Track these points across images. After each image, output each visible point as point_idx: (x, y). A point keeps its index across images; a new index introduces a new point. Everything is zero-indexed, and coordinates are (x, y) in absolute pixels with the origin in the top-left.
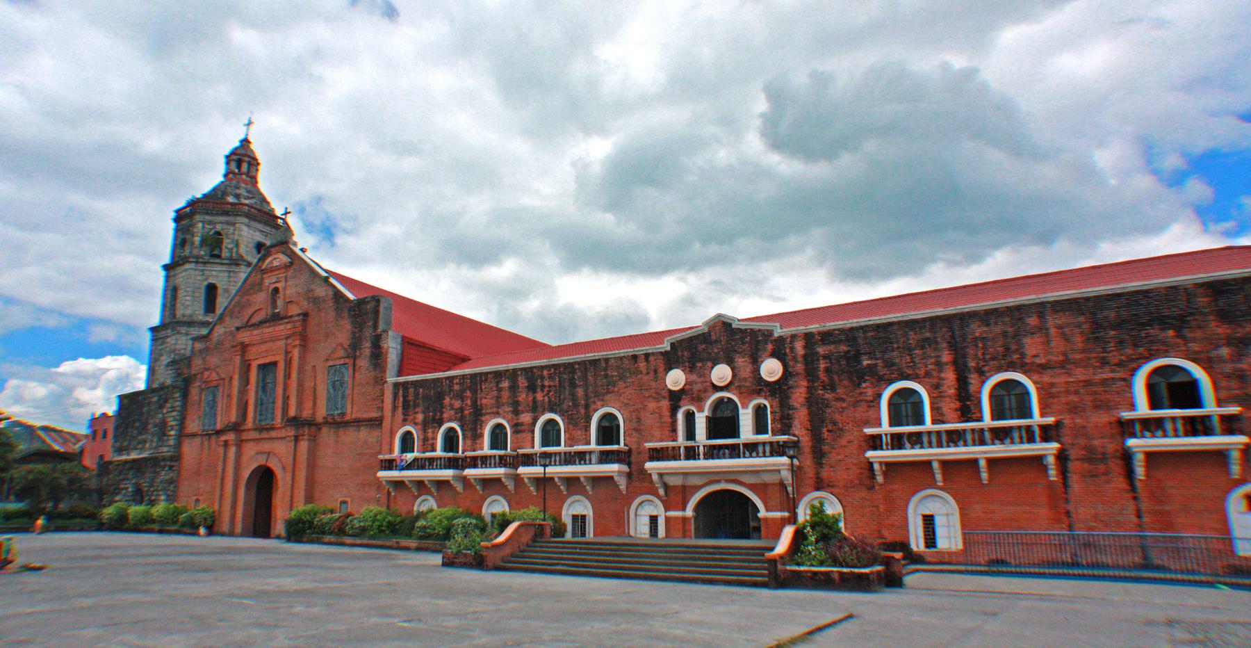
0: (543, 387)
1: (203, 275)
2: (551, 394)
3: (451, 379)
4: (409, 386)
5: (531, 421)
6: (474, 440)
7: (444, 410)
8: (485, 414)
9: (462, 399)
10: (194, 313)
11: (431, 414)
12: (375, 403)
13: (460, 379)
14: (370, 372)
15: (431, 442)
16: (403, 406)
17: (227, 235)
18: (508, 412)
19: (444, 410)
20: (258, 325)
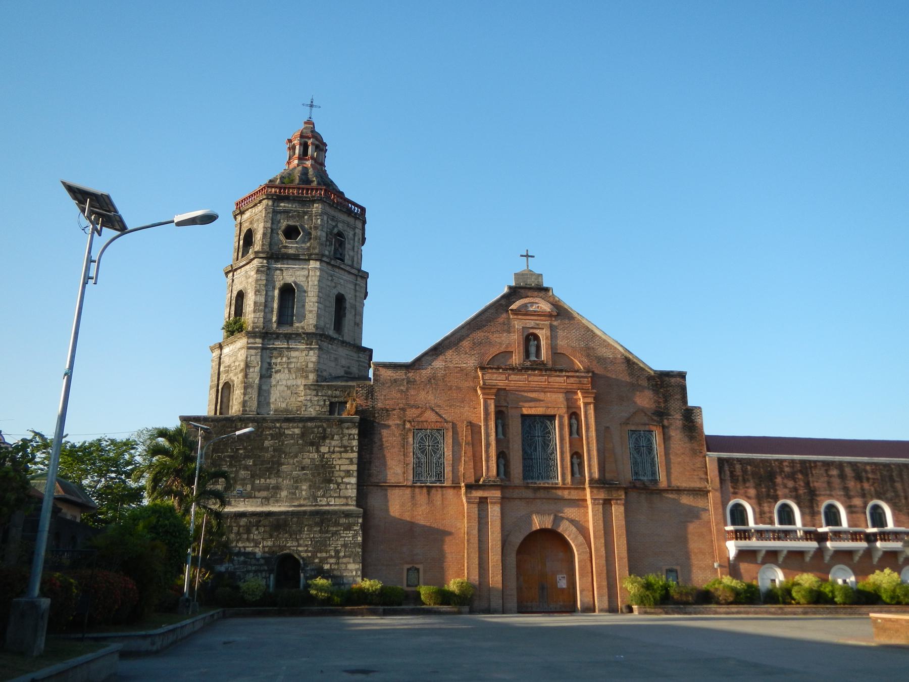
0: (868, 479)
1: (332, 280)
2: (876, 485)
3: (781, 461)
4: (735, 462)
5: (862, 505)
6: (812, 516)
7: (777, 488)
8: (820, 495)
9: (795, 480)
10: (325, 326)
11: (764, 490)
12: (696, 473)
13: (789, 463)
14: (685, 443)
15: (768, 515)
16: (731, 480)
17: (348, 238)
18: (841, 495)
19: (777, 488)
20: (521, 370)
